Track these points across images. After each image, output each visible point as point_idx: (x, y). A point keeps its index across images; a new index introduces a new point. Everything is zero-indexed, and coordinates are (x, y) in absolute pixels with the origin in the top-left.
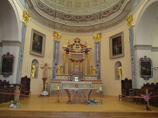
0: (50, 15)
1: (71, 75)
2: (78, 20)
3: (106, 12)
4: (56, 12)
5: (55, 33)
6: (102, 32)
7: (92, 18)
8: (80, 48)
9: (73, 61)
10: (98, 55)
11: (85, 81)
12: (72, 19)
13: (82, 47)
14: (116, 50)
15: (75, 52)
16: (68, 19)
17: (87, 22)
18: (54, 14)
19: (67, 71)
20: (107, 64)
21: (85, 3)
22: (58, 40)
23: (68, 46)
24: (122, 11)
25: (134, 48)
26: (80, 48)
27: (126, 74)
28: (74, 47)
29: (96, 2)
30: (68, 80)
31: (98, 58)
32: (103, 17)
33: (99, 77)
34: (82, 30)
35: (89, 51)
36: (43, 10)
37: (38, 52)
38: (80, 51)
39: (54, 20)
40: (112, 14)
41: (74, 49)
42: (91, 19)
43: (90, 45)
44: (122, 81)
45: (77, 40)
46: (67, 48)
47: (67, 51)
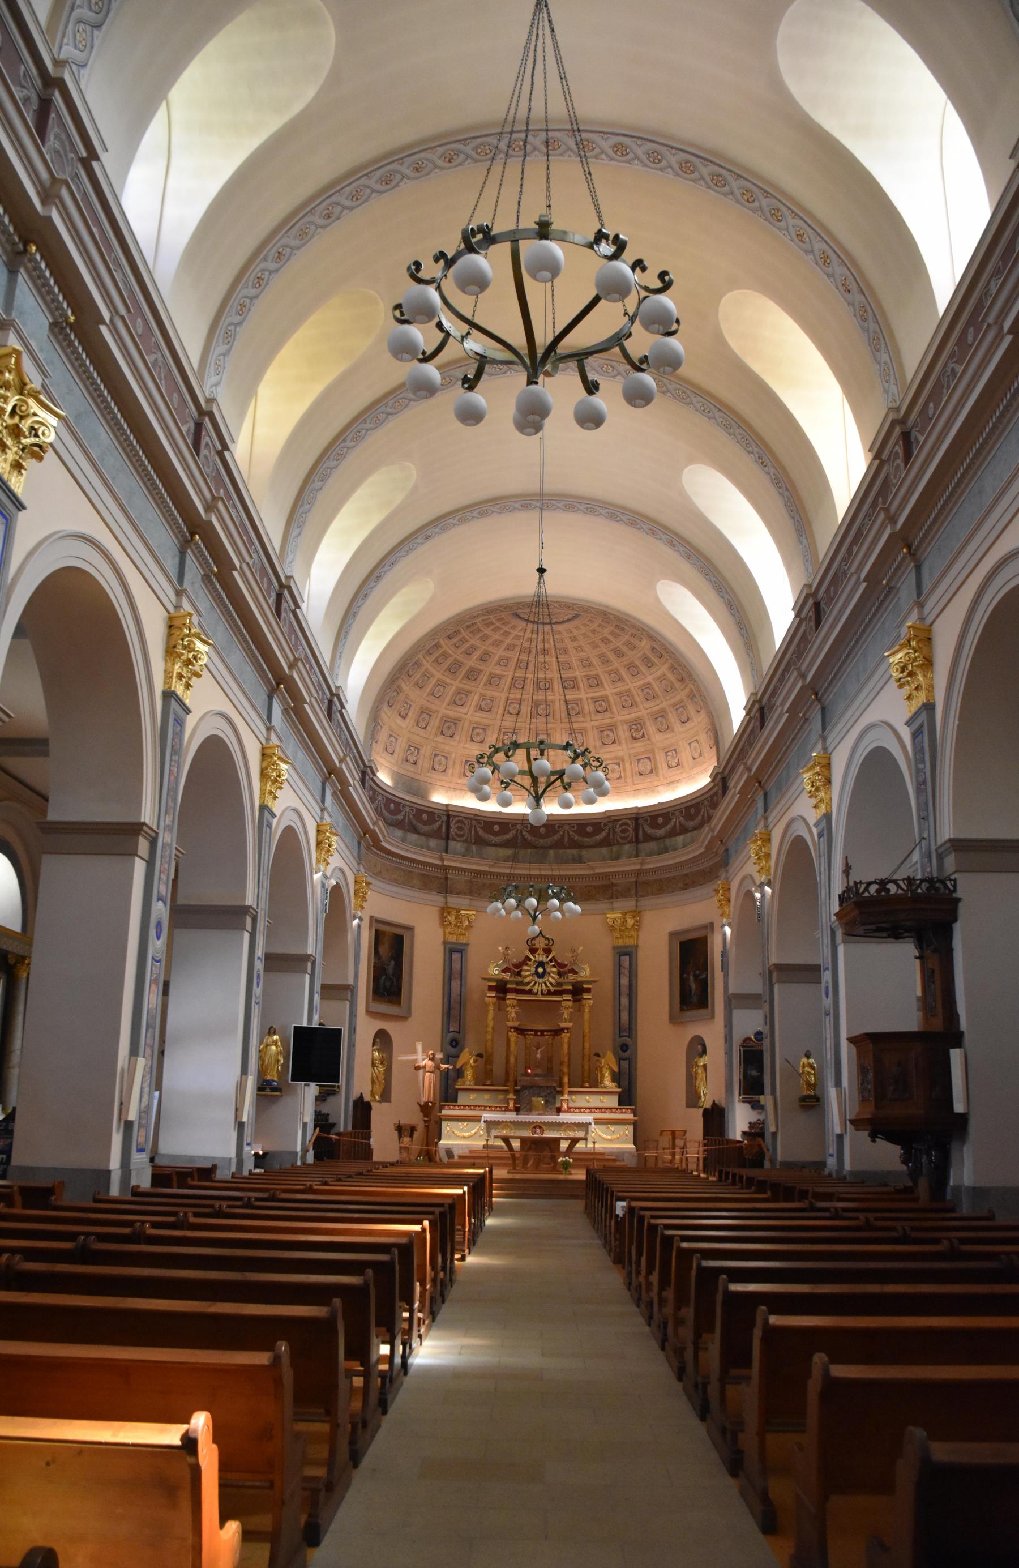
0: (428, 835)
1: (518, 1088)
3: (660, 820)
4: (449, 816)
7: (604, 834)
8: (552, 978)
9: (521, 1031)
10: (625, 1001)
11: (569, 1110)
12: (515, 837)
13: (559, 974)
14: (691, 990)
15: (530, 992)
17: (584, 852)
19: (498, 1069)
22: (463, 940)
23: (503, 971)
24: (702, 850)
25: (733, 1001)
26: (552, 978)
27: (710, 1093)
28: (528, 970)
29: (618, 764)
30: (507, 1109)
31: (625, 1016)
32: (649, 838)
35: (588, 991)
36: (398, 825)
37: (390, 1002)
38: (552, 989)
39: (442, 860)
40: (682, 837)
41: (527, 980)
44: (706, 1112)
45: (540, 944)
46: (498, 981)
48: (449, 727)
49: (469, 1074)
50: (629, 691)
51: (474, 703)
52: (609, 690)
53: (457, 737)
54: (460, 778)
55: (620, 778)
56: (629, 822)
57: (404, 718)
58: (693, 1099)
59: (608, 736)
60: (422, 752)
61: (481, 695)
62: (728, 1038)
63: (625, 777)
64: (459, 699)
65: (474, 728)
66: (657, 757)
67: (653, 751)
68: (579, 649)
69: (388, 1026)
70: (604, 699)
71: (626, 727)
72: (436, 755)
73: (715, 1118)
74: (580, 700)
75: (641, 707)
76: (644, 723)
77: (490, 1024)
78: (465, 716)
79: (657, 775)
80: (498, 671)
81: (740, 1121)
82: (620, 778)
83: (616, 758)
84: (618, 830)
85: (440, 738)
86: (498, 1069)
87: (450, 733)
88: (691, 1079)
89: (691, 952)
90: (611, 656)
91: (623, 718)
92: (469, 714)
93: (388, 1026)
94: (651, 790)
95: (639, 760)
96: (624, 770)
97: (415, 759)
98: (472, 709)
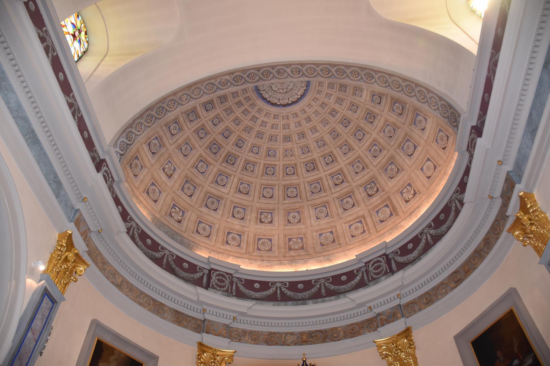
2: (300, 295)
5: (204, 352)
7: (358, 278)
16: (258, 295)
18: (202, 277)
21: (320, 235)
29: (361, 222)
34: (321, 331)
42: (353, 283)
48: (212, 202)
50: (359, 157)
51: (234, 186)
52: (343, 162)
53: (220, 212)
54: (223, 245)
55: (364, 231)
56: (381, 259)
57: (170, 176)
59: (347, 202)
60: (187, 215)
61: (240, 179)
63: (369, 229)
64: (220, 179)
65: (235, 207)
66: (394, 201)
67: (389, 198)
68: (314, 130)
70: (340, 172)
71: (361, 189)
72: (200, 222)
74: (321, 179)
75: (371, 166)
76: (376, 179)
78: (226, 196)
79: (397, 214)
80: (252, 157)
82: (364, 231)
83: (357, 218)
84: (371, 269)
85: (205, 210)
87: (214, 207)
90: (340, 128)
91: (359, 182)
92: (228, 193)
94: (395, 227)
95: (377, 212)
96: (367, 224)
97: (180, 218)
98: (233, 190)
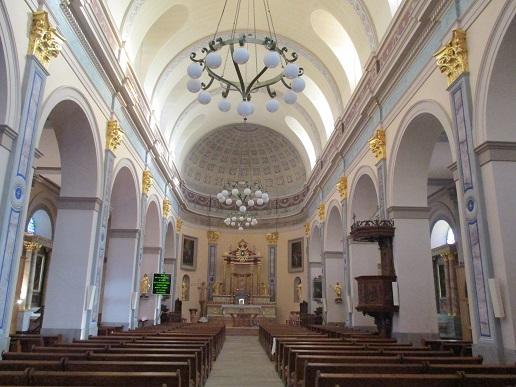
6: (279, 230)
9: (235, 275)
17: (259, 212)
19: (228, 289)
20: (284, 277)
27: (303, 297)
28: (238, 254)
33: (273, 299)
43: (262, 252)
47: (229, 260)
49: (217, 291)
58: (297, 298)
62: (309, 277)
69: (188, 273)
73: (304, 306)
77: (224, 274)
81: (313, 307)
86: (228, 289)
88: (296, 293)
89: (296, 248)
93: (188, 273)
